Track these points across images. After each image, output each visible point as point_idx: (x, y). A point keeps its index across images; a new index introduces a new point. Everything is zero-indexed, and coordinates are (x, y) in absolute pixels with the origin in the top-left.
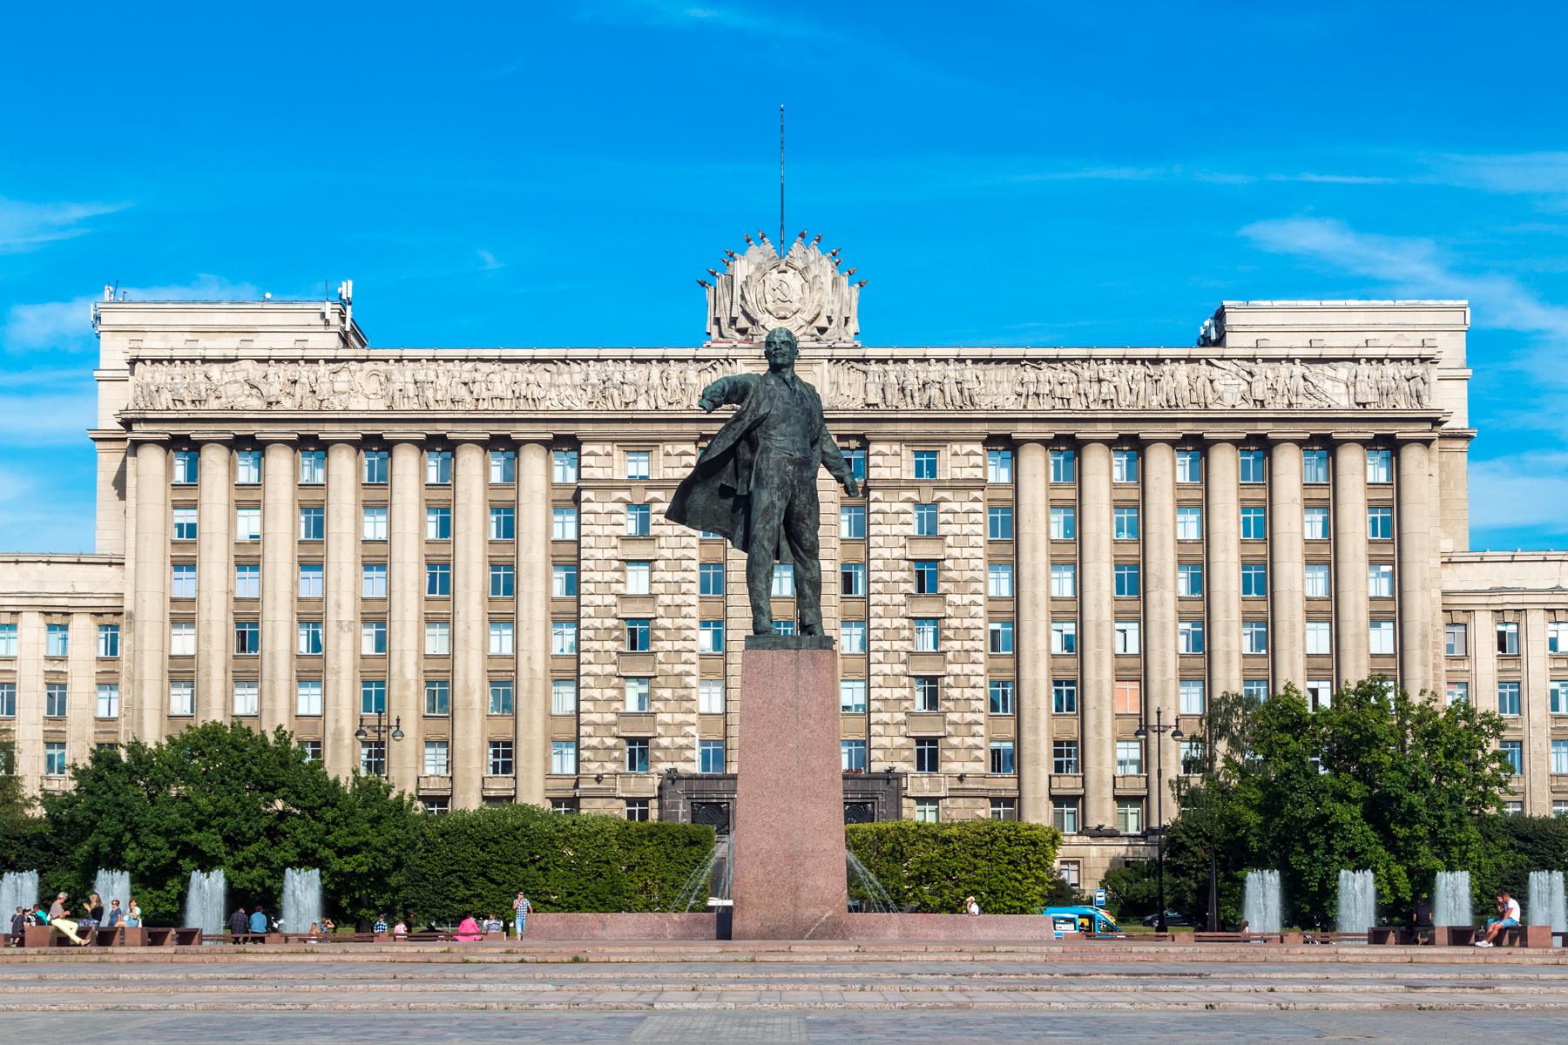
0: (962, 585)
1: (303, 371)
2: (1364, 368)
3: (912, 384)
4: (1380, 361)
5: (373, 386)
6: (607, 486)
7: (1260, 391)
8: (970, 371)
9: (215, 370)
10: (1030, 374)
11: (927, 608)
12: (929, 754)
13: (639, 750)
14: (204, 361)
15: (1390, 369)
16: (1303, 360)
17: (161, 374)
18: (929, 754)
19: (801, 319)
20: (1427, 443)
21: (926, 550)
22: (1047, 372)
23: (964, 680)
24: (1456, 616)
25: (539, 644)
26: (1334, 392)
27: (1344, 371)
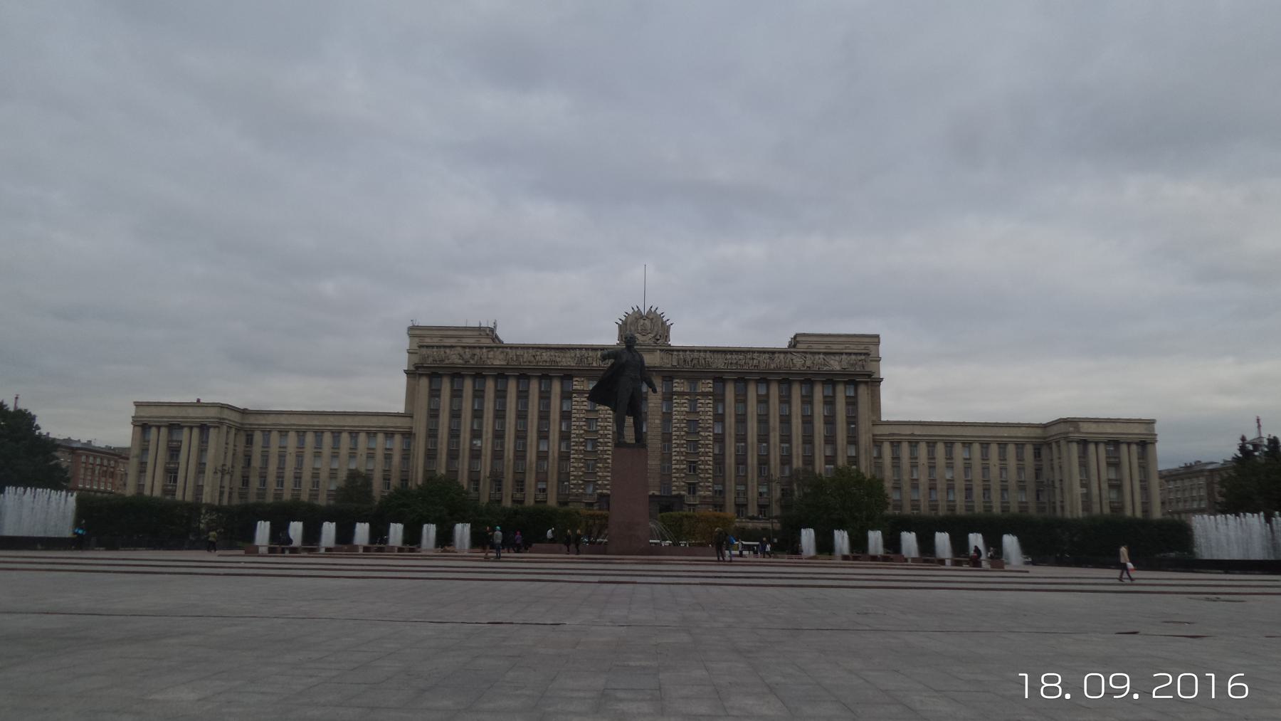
0: (706, 429)
1: (477, 351)
2: (844, 357)
3: (689, 359)
4: (850, 354)
5: (502, 356)
7: (808, 363)
8: (708, 355)
9: (448, 351)
10: (729, 356)
12: (692, 488)
14: (445, 347)
15: (853, 357)
16: (825, 354)
17: (429, 351)
18: (692, 488)
19: (651, 336)
20: (866, 383)
21: (692, 417)
22: (734, 356)
23: (705, 463)
24: (877, 443)
25: (556, 447)
26: (835, 365)
27: (837, 358)
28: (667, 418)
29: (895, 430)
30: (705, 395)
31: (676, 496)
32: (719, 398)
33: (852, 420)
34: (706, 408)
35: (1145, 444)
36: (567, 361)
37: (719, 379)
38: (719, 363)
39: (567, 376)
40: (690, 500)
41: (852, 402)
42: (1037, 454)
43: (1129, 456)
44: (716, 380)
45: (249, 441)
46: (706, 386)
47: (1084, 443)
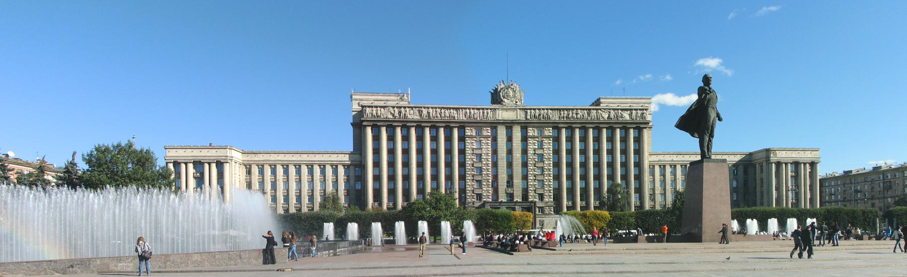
6: (471, 137)
11: (540, 165)
13: (479, 197)
16: (622, 110)
18: (541, 197)
28: (525, 152)
29: (661, 157)
30: (548, 137)
31: (532, 202)
32: (557, 139)
33: (639, 152)
34: (549, 145)
35: (813, 164)
36: (461, 116)
37: (556, 127)
38: (555, 117)
39: (462, 126)
40: (539, 204)
41: (638, 140)
42: (746, 172)
43: (805, 171)
44: (554, 128)
45: (249, 172)
46: (549, 132)
47: (779, 164)
